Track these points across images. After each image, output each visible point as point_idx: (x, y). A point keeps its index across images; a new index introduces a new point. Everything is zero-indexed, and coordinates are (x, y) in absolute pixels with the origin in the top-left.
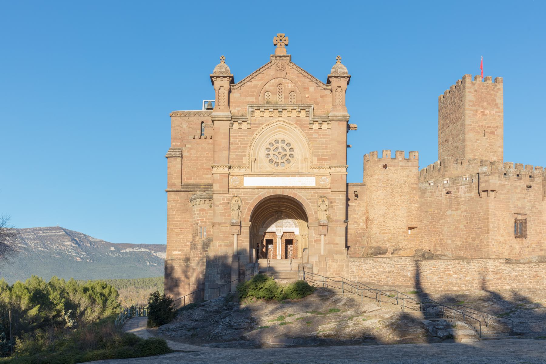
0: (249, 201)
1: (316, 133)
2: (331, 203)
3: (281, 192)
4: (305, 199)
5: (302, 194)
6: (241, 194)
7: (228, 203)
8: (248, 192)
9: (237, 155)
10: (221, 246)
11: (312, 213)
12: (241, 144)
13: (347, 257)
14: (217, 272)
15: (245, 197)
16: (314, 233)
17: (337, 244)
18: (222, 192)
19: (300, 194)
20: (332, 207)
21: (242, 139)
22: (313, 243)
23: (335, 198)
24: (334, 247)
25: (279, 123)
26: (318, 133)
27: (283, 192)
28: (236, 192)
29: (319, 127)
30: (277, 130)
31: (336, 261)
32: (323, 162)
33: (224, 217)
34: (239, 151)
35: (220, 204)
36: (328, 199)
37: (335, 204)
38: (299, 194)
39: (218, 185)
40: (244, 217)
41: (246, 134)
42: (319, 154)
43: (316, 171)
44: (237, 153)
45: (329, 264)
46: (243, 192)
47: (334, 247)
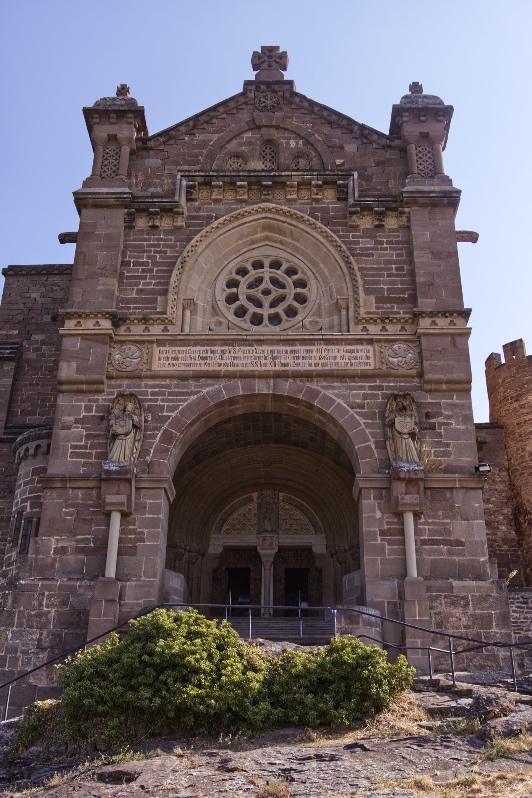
0: (169, 414)
1: (368, 237)
2: (428, 416)
3: (268, 389)
4: (347, 406)
5: (336, 391)
6: (146, 393)
7: (102, 418)
8: (168, 387)
9: (140, 291)
10: (62, 551)
11: (369, 446)
12: (155, 264)
13: (501, 588)
14: (39, 640)
15: (157, 400)
16: (380, 509)
17: (458, 543)
18: (84, 387)
19: (329, 393)
20: (433, 427)
21: (160, 252)
22: (376, 540)
23: (439, 403)
24: (450, 553)
25: (264, 215)
26: (373, 237)
27: (274, 386)
28: (128, 386)
29: (377, 223)
30: (259, 235)
31: (462, 602)
32: (393, 307)
33: (83, 460)
34: (148, 281)
35: (77, 421)
36: (419, 406)
37: (441, 420)
38: (323, 391)
39: (74, 365)
40: (148, 458)
41: (170, 240)
42: (382, 286)
43: (374, 330)
44: (140, 287)
45: (439, 613)
46: (153, 386)
47: (450, 553)
